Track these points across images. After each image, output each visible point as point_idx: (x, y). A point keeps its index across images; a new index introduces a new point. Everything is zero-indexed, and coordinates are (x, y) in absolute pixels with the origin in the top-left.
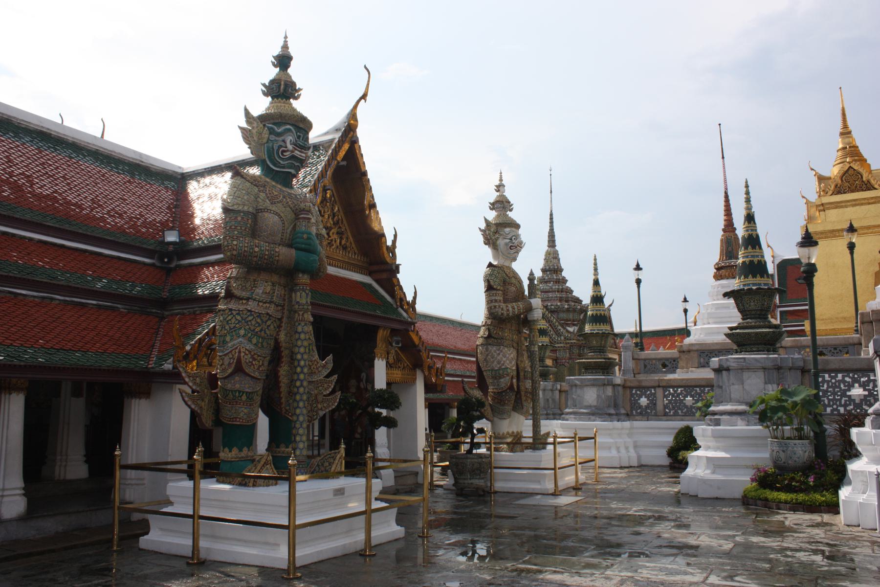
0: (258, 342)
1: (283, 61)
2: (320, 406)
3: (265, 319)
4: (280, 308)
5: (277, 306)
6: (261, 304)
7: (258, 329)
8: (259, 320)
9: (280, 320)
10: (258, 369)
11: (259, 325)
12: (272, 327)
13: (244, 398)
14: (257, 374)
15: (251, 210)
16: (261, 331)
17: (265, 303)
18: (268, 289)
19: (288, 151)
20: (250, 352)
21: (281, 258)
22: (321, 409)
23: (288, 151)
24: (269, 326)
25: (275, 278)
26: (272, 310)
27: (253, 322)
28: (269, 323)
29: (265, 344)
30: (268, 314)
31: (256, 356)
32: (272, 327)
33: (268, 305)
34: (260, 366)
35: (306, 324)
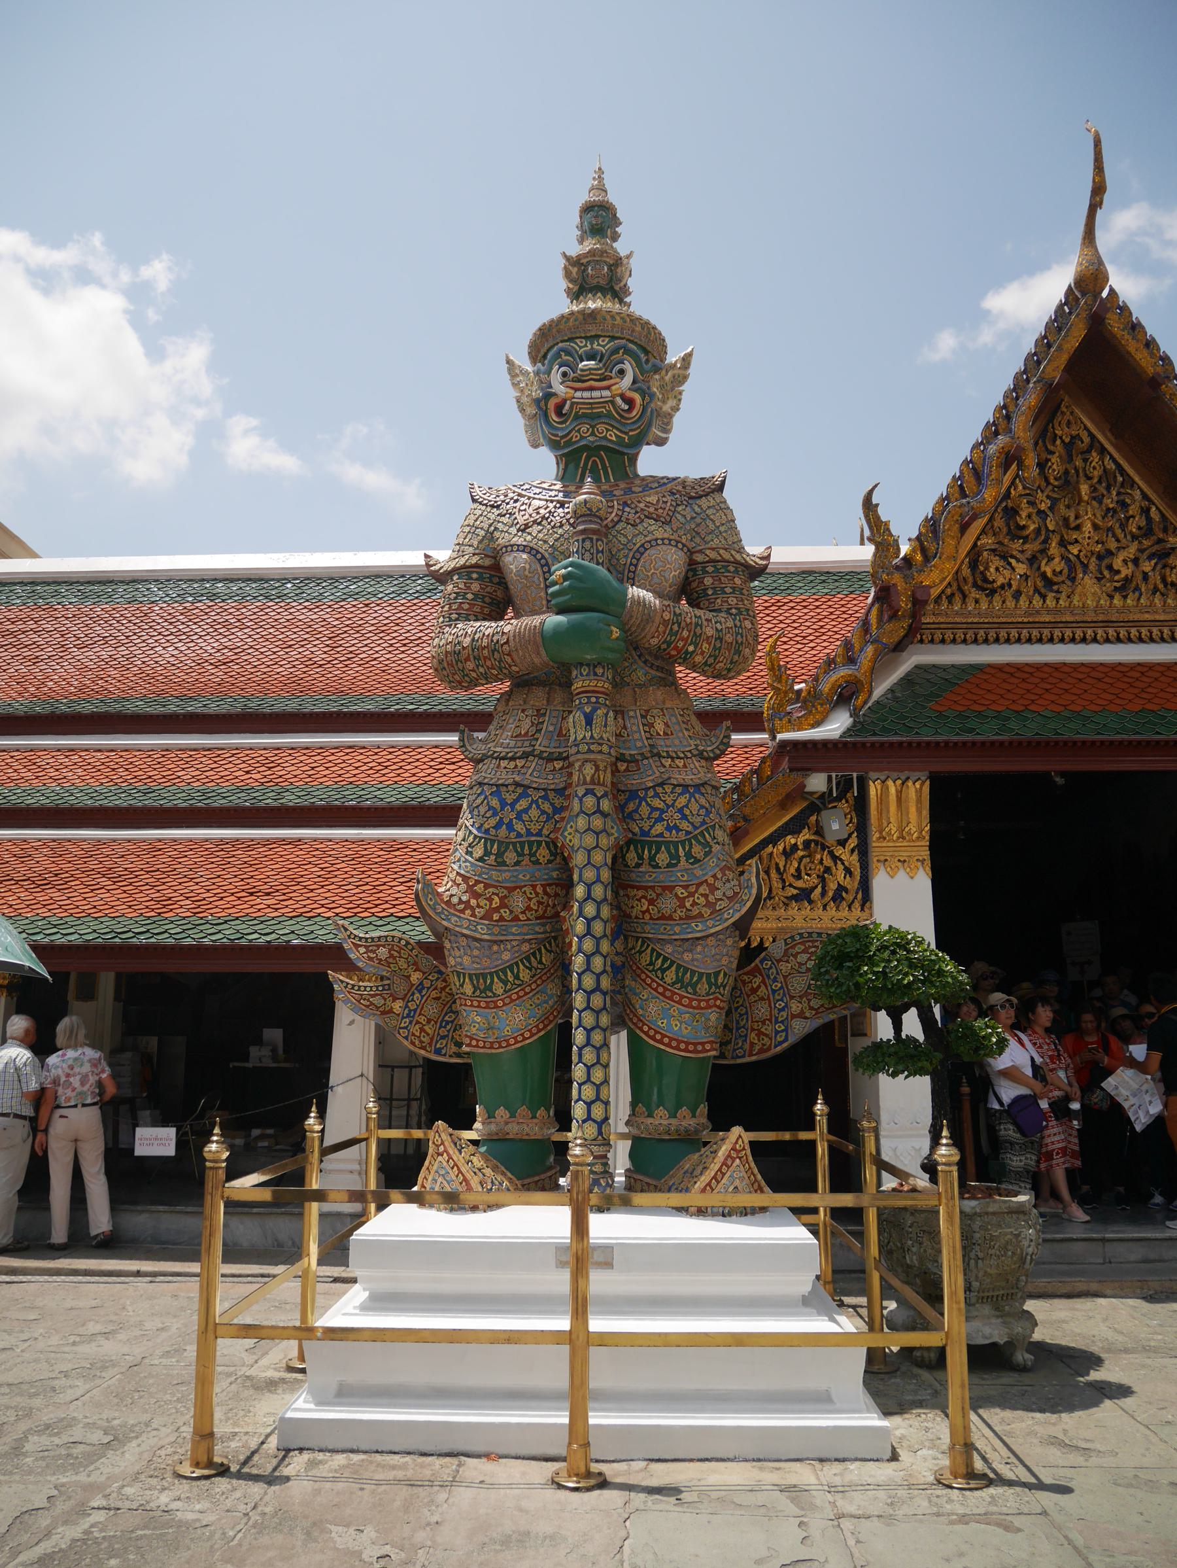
0: (487, 853)
1: (599, 218)
2: (795, 1007)
3: (509, 798)
4: (558, 765)
5: (550, 759)
6: (504, 763)
7: (493, 822)
8: (495, 802)
9: (560, 792)
10: (487, 916)
11: (495, 814)
12: (534, 812)
13: (468, 989)
14: (482, 931)
15: (474, 560)
16: (497, 826)
17: (513, 759)
18: (526, 725)
19: (564, 401)
20: (465, 879)
21: (512, 643)
22: (801, 1015)
23: (564, 401)
24: (526, 811)
25: (538, 697)
26: (532, 773)
27: (483, 809)
28: (522, 804)
29: (510, 857)
30: (517, 784)
31: (479, 888)
32: (534, 812)
33: (520, 763)
34: (497, 910)
35: (589, 792)
